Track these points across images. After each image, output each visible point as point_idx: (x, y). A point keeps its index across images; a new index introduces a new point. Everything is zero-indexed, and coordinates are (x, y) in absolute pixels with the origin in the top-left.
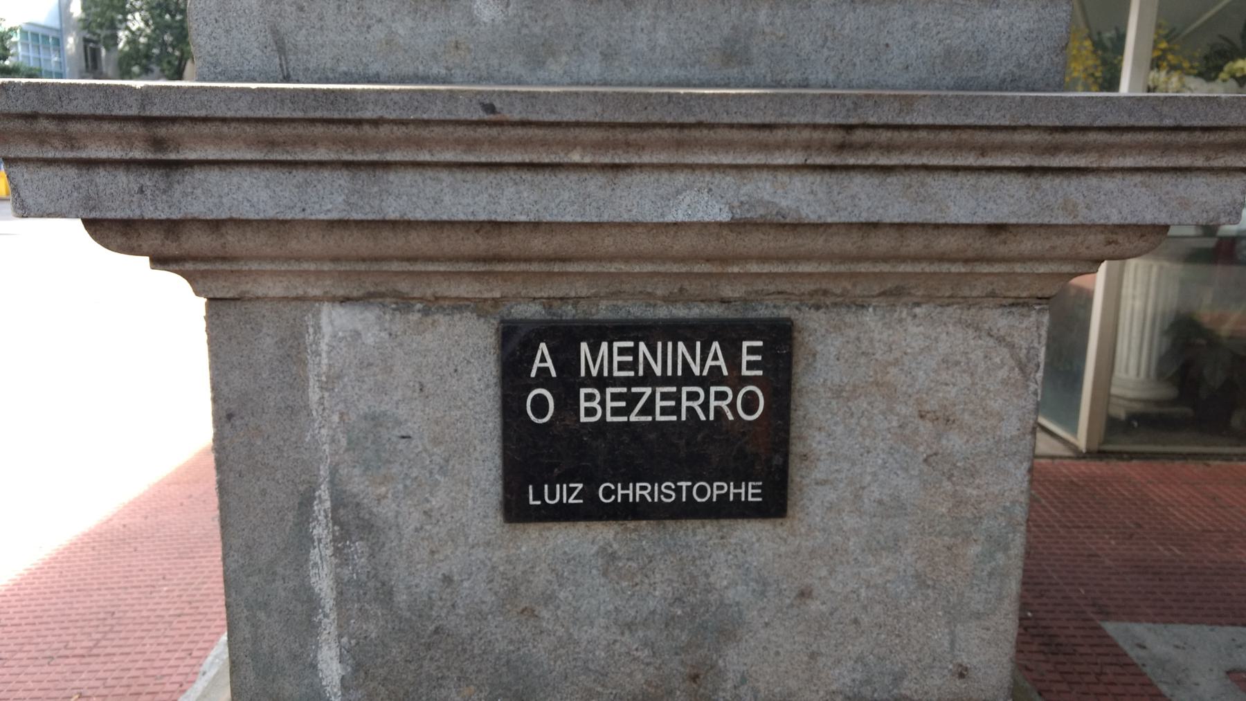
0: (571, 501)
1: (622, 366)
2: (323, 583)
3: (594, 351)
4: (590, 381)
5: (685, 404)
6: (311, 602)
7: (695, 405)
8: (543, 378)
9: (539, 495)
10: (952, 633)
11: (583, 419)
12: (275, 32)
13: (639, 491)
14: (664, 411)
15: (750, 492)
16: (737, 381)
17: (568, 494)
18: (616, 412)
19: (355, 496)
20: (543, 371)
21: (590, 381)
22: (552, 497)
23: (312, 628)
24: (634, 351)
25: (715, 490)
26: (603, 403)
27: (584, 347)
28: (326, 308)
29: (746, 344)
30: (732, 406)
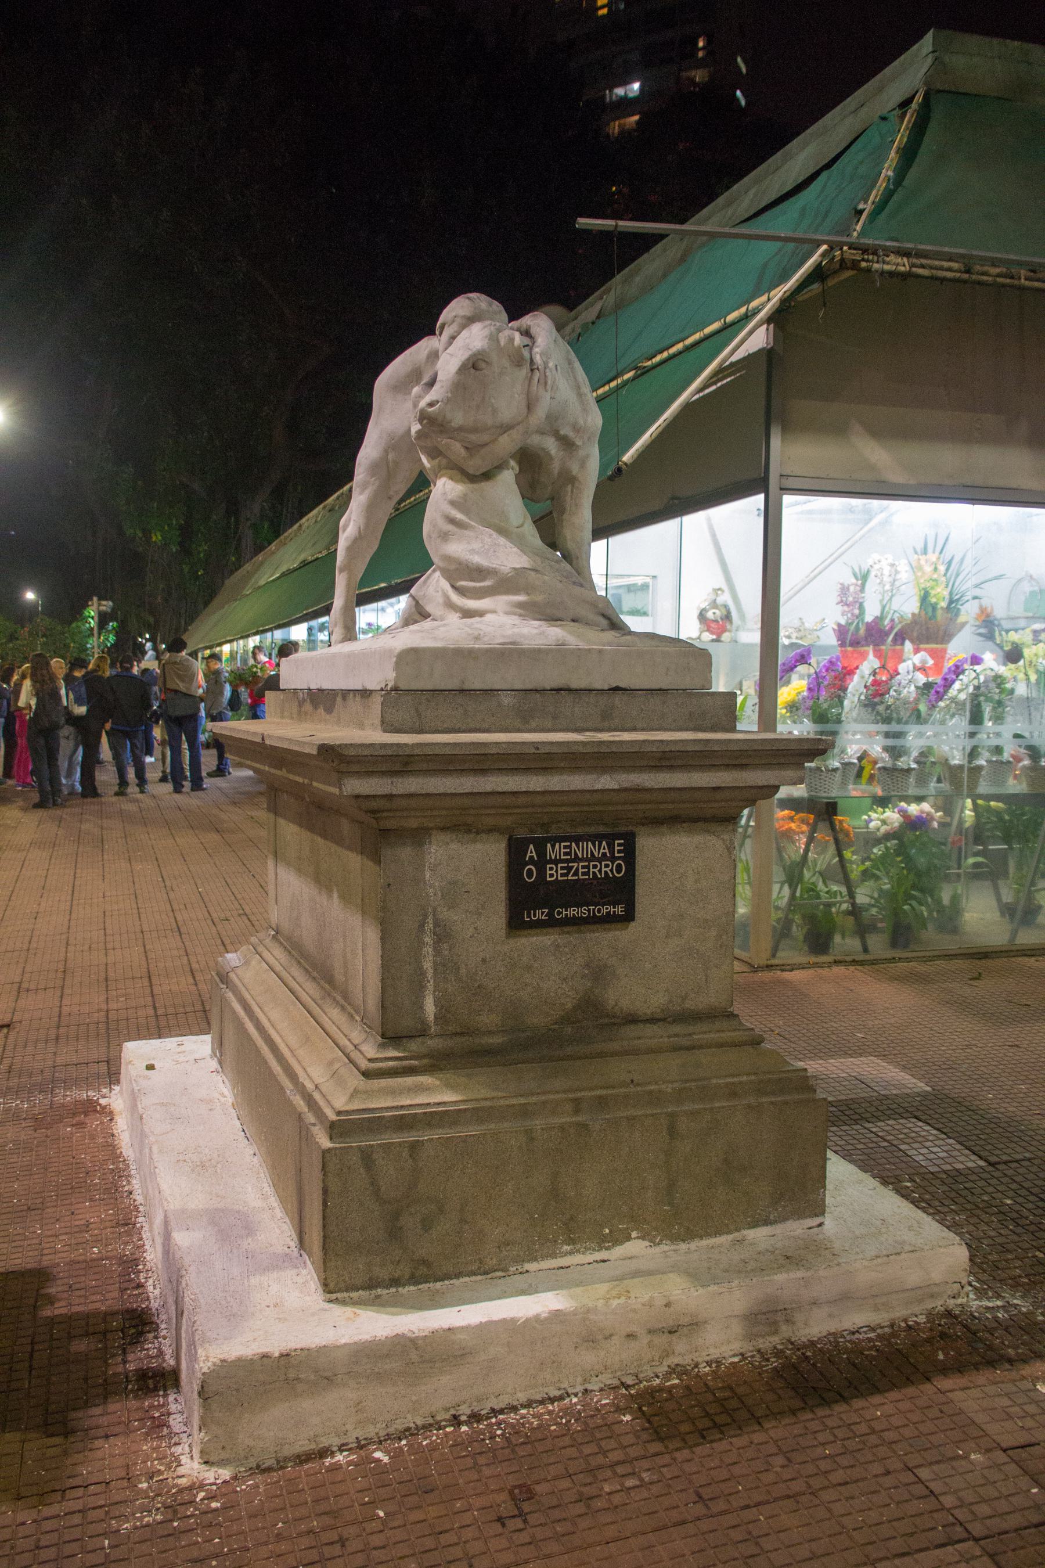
1: (565, 854)
2: (428, 965)
3: (553, 847)
4: (551, 861)
5: (592, 870)
6: (423, 973)
7: (596, 870)
8: (531, 861)
9: (529, 916)
10: (706, 975)
11: (548, 879)
13: (572, 912)
14: (583, 874)
15: (619, 910)
16: (613, 859)
17: (541, 915)
18: (562, 875)
20: (531, 857)
21: (551, 861)
22: (535, 916)
23: (422, 988)
24: (570, 847)
25: (605, 910)
26: (557, 871)
27: (549, 845)
28: (434, 832)
30: (611, 870)
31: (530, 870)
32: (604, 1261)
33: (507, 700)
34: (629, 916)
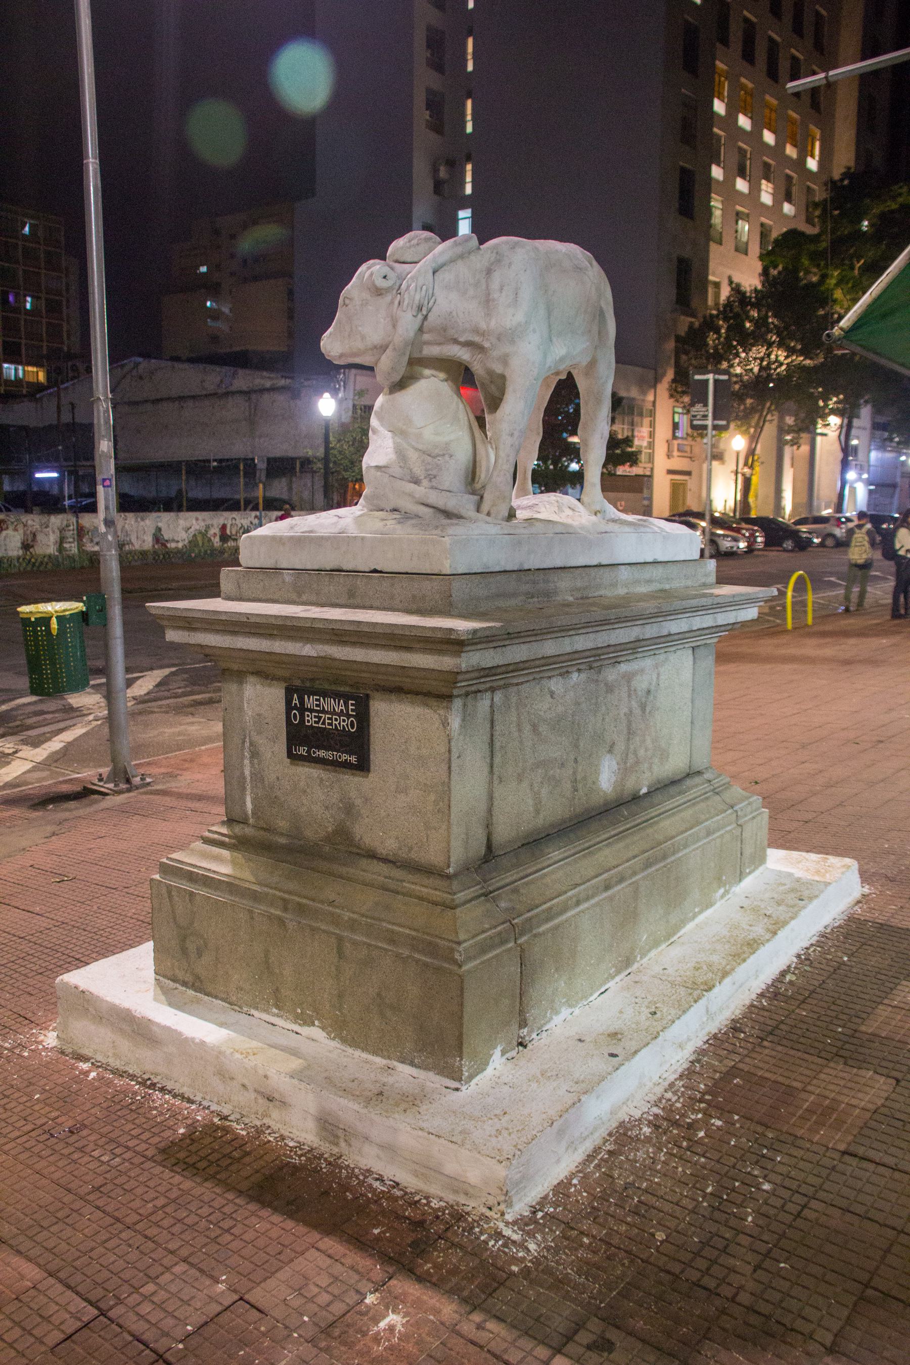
1: (317, 705)
2: (247, 772)
6: (244, 778)
13: (322, 753)
15: (353, 759)
16: (349, 716)
18: (315, 722)
23: (244, 789)
32: (297, 1033)
33: (288, 577)
34: (363, 766)
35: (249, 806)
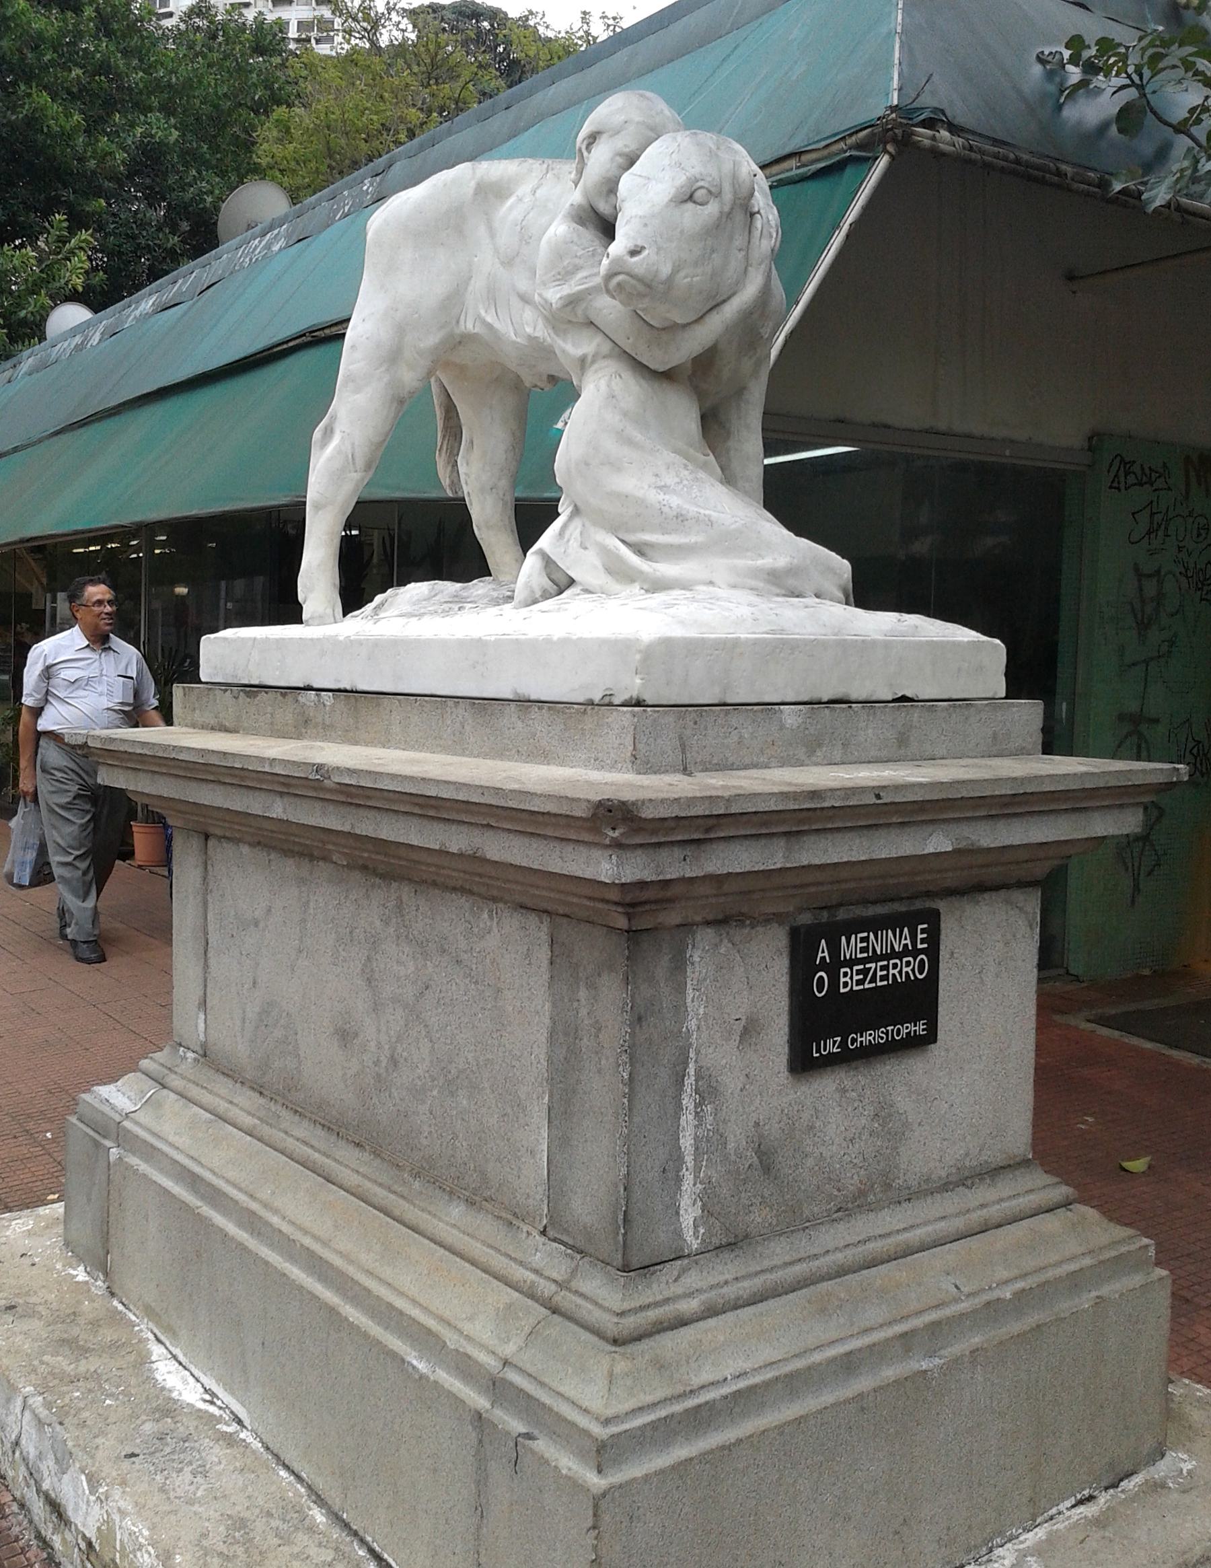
0: (835, 1050)
1: (863, 950)
5: (891, 972)
8: (823, 966)
9: (818, 1051)
11: (842, 990)
12: (681, 738)
14: (883, 978)
15: (920, 1028)
17: (832, 1046)
18: (859, 982)
19: (708, 1069)
26: (851, 978)
27: (843, 938)
29: (920, 927)
30: (913, 970)
31: (821, 978)
34: (931, 1037)
35: (689, 1214)
